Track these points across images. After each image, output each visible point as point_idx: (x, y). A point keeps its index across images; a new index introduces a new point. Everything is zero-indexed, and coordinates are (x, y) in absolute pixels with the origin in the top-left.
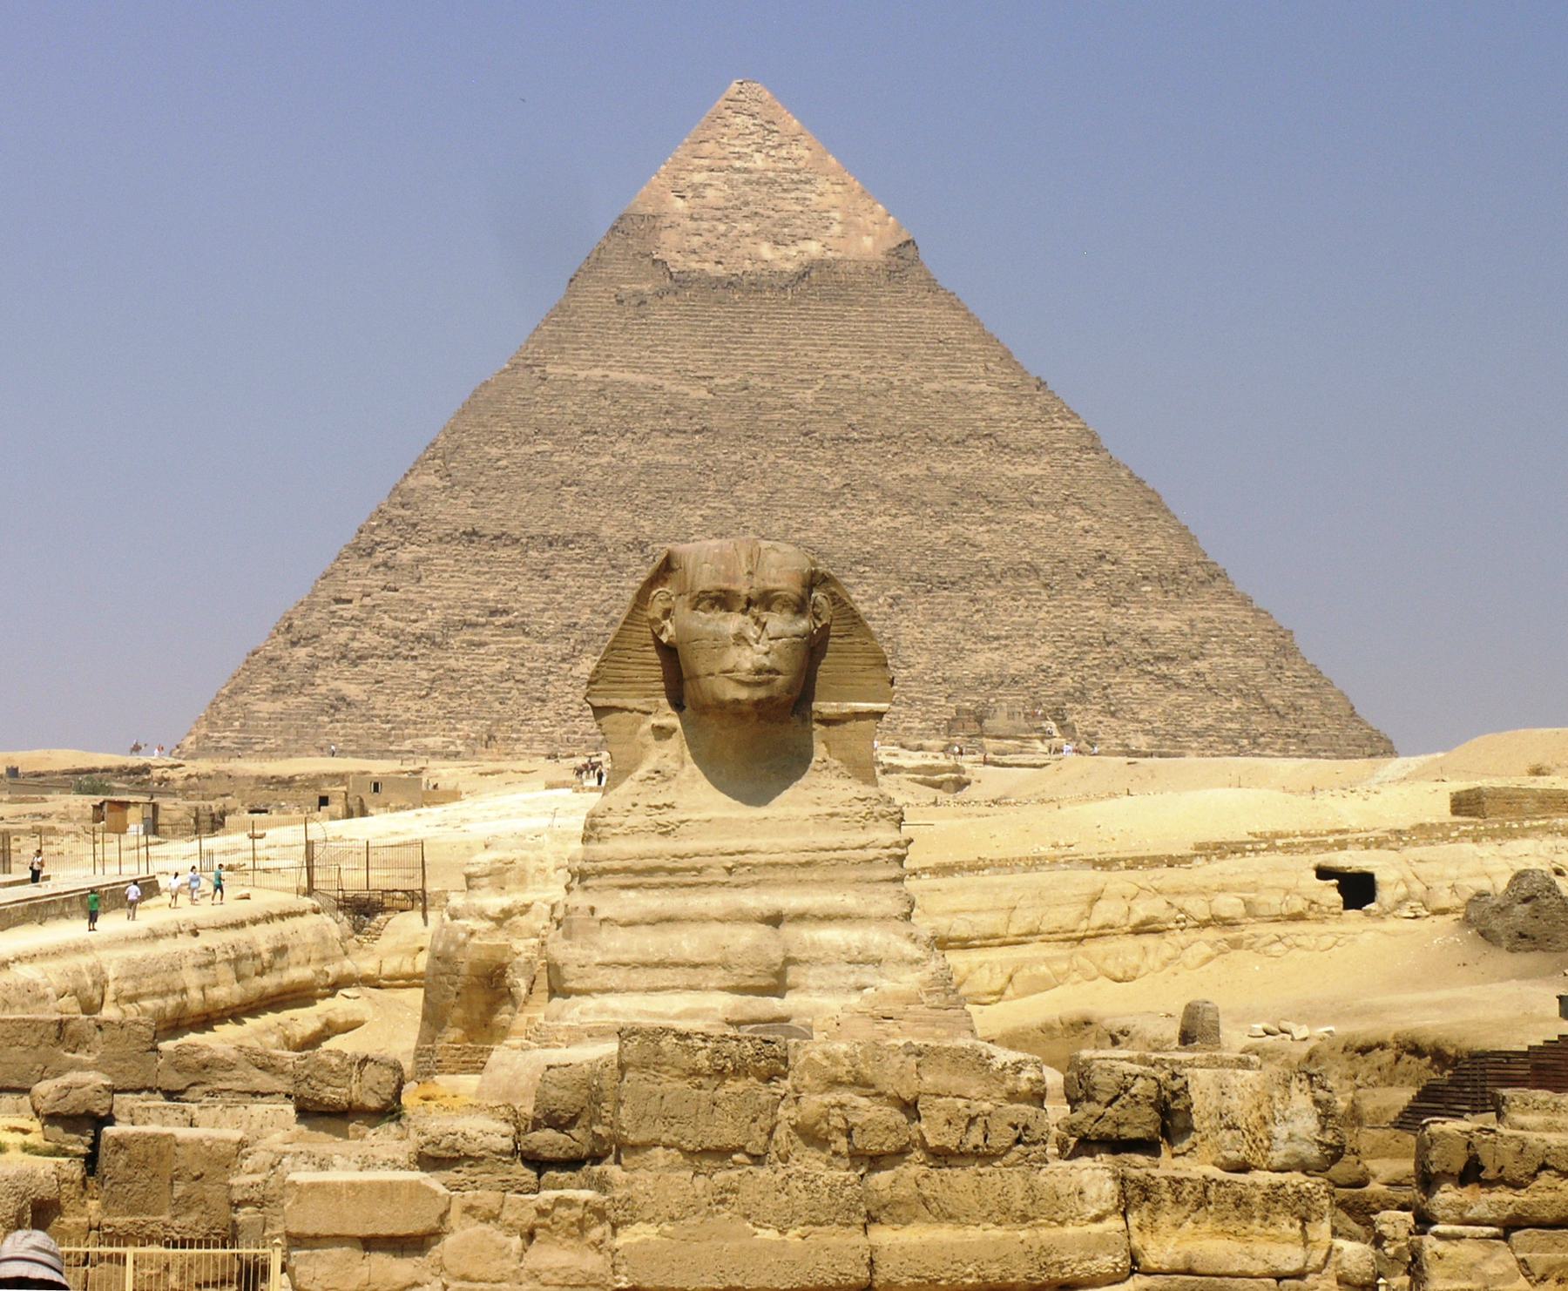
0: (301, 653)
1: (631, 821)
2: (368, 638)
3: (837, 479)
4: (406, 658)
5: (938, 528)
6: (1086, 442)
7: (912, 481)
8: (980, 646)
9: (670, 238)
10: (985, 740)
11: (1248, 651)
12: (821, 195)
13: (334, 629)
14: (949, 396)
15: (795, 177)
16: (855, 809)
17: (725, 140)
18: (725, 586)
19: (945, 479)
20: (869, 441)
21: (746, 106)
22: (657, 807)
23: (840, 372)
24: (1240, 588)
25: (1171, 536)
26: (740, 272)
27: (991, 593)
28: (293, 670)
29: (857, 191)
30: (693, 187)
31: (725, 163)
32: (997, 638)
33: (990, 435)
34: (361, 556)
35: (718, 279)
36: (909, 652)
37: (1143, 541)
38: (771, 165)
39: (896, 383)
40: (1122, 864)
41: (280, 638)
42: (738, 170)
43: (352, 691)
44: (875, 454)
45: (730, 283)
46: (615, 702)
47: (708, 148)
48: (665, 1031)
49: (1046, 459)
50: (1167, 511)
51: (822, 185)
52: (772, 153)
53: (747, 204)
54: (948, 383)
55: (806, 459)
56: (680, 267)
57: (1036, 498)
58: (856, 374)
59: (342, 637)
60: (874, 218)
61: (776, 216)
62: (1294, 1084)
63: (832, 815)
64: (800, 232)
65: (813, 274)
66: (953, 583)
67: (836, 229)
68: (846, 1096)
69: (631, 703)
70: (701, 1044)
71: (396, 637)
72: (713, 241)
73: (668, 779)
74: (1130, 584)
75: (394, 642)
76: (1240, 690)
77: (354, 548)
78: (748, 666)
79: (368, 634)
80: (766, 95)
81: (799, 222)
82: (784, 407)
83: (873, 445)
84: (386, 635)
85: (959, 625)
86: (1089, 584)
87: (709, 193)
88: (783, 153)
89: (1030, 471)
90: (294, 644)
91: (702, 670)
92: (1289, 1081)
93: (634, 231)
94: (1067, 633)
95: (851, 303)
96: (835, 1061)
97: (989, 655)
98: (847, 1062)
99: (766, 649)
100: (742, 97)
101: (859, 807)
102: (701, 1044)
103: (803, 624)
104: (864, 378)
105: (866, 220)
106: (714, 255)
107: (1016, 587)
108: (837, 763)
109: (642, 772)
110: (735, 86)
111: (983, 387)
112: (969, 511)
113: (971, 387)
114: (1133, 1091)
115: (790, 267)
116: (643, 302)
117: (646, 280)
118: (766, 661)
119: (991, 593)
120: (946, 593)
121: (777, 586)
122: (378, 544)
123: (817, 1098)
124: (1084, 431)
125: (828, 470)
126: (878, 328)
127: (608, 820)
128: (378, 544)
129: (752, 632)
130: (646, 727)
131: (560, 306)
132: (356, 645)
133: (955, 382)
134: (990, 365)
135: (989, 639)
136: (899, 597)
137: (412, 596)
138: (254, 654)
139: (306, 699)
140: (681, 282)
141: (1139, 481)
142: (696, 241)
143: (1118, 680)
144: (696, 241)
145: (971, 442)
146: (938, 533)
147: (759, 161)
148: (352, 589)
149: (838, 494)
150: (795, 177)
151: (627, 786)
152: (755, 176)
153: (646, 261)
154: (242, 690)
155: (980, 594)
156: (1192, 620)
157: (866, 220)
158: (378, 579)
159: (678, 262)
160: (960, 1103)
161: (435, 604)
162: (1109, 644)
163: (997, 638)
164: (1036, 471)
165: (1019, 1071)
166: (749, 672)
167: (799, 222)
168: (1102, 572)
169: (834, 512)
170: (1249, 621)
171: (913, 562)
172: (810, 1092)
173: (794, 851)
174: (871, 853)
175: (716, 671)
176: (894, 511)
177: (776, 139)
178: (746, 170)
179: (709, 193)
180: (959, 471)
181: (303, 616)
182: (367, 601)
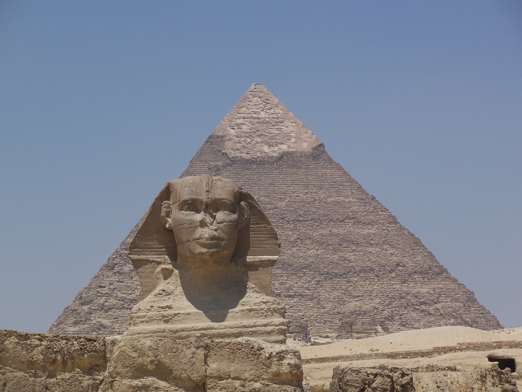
0: (86, 308)
1: (150, 314)
2: (112, 301)
3: (295, 236)
4: (127, 309)
5: (334, 254)
6: (391, 220)
7: (324, 236)
8: (351, 300)
9: (228, 144)
10: (353, 334)
11: (457, 300)
12: (287, 127)
13: (99, 298)
14: (337, 203)
15: (277, 120)
16: (261, 307)
17: (249, 107)
18: (194, 197)
19: (338, 235)
20: (307, 221)
21: (258, 93)
22: (163, 308)
23: (295, 195)
24: (452, 275)
25: (425, 256)
26: (256, 157)
27: (355, 279)
28: (82, 314)
29: (301, 126)
30: (237, 125)
31: (250, 115)
32: (358, 297)
33: (354, 218)
34: (109, 269)
35: (248, 160)
36: (324, 302)
37: (414, 258)
38: (268, 116)
39: (317, 198)
40: (401, 356)
41: (77, 302)
42: (255, 118)
43: (106, 322)
44: (309, 226)
45: (252, 161)
46: (143, 257)
47: (243, 110)
48: (10, 334)
49: (376, 226)
50: (424, 246)
51: (287, 123)
52: (268, 111)
53: (258, 131)
54: (337, 198)
55: (283, 228)
56: (233, 155)
57: (372, 242)
58: (301, 195)
59: (102, 300)
60: (308, 135)
61: (270, 135)
62: (489, 379)
63: (250, 310)
64: (279, 141)
65: (284, 157)
66: (341, 276)
67: (293, 140)
68: (149, 380)
69: (151, 257)
70: (37, 342)
71: (123, 301)
72: (246, 145)
73: (169, 294)
74: (410, 275)
75: (122, 302)
76: (454, 316)
77: (107, 266)
78: (207, 236)
79: (112, 300)
80: (265, 89)
81: (279, 137)
82: (273, 209)
83: (308, 222)
84: (119, 300)
85: (343, 291)
86: (393, 275)
87: (244, 127)
88: (272, 111)
89: (370, 231)
90: (83, 304)
91: (184, 239)
92: (485, 377)
93: (215, 142)
94: (385, 294)
95: (299, 168)
96: (143, 354)
97: (355, 303)
98: (150, 353)
99: (216, 228)
100: (256, 90)
101: (263, 306)
102: (37, 342)
103: (235, 216)
104: (305, 197)
105: (304, 136)
106: (245, 151)
107: (365, 277)
108: (253, 286)
109: (156, 291)
110: (253, 86)
111: (351, 199)
112: (346, 247)
113: (346, 200)
114: (374, 385)
115: (275, 155)
116: (218, 169)
117: (220, 160)
118: (215, 233)
119: (355, 279)
120: (338, 279)
121: (221, 197)
122: (116, 264)
123: (127, 382)
124: (391, 216)
125: (292, 232)
126: (310, 178)
127: (139, 314)
128: (116, 264)
129: (208, 219)
130: (159, 269)
131: (186, 171)
132: (107, 304)
133: (340, 198)
134: (353, 191)
135: (355, 297)
136: (320, 281)
137: (129, 284)
138: (67, 308)
139: (88, 326)
140: (234, 161)
141: (413, 235)
142: (239, 146)
143: (406, 312)
144: (239, 146)
145: (347, 221)
146: (334, 256)
147: (263, 115)
148: (106, 282)
149: (295, 241)
150: (277, 120)
151: (149, 298)
152: (261, 120)
153: (219, 154)
154: (62, 323)
155: (351, 279)
156: (434, 288)
157: (304, 136)
158: (115, 278)
159: (232, 154)
160: (237, 383)
161: (138, 287)
162: (402, 298)
163: (358, 297)
164: (372, 231)
165: (282, 358)
166: (207, 239)
167: (279, 137)
168: (399, 270)
169: (294, 249)
170: (457, 288)
171: (325, 268)
172: (123, 377)
173: (230, 328)
174: (269, 328)
175: (191, 239)
176: (317, 248)
177: (269, 106)
178: (258, 118)
179: (244, 127)
180: (342, 232)
181: (86, 293)
182: (111, 286)
